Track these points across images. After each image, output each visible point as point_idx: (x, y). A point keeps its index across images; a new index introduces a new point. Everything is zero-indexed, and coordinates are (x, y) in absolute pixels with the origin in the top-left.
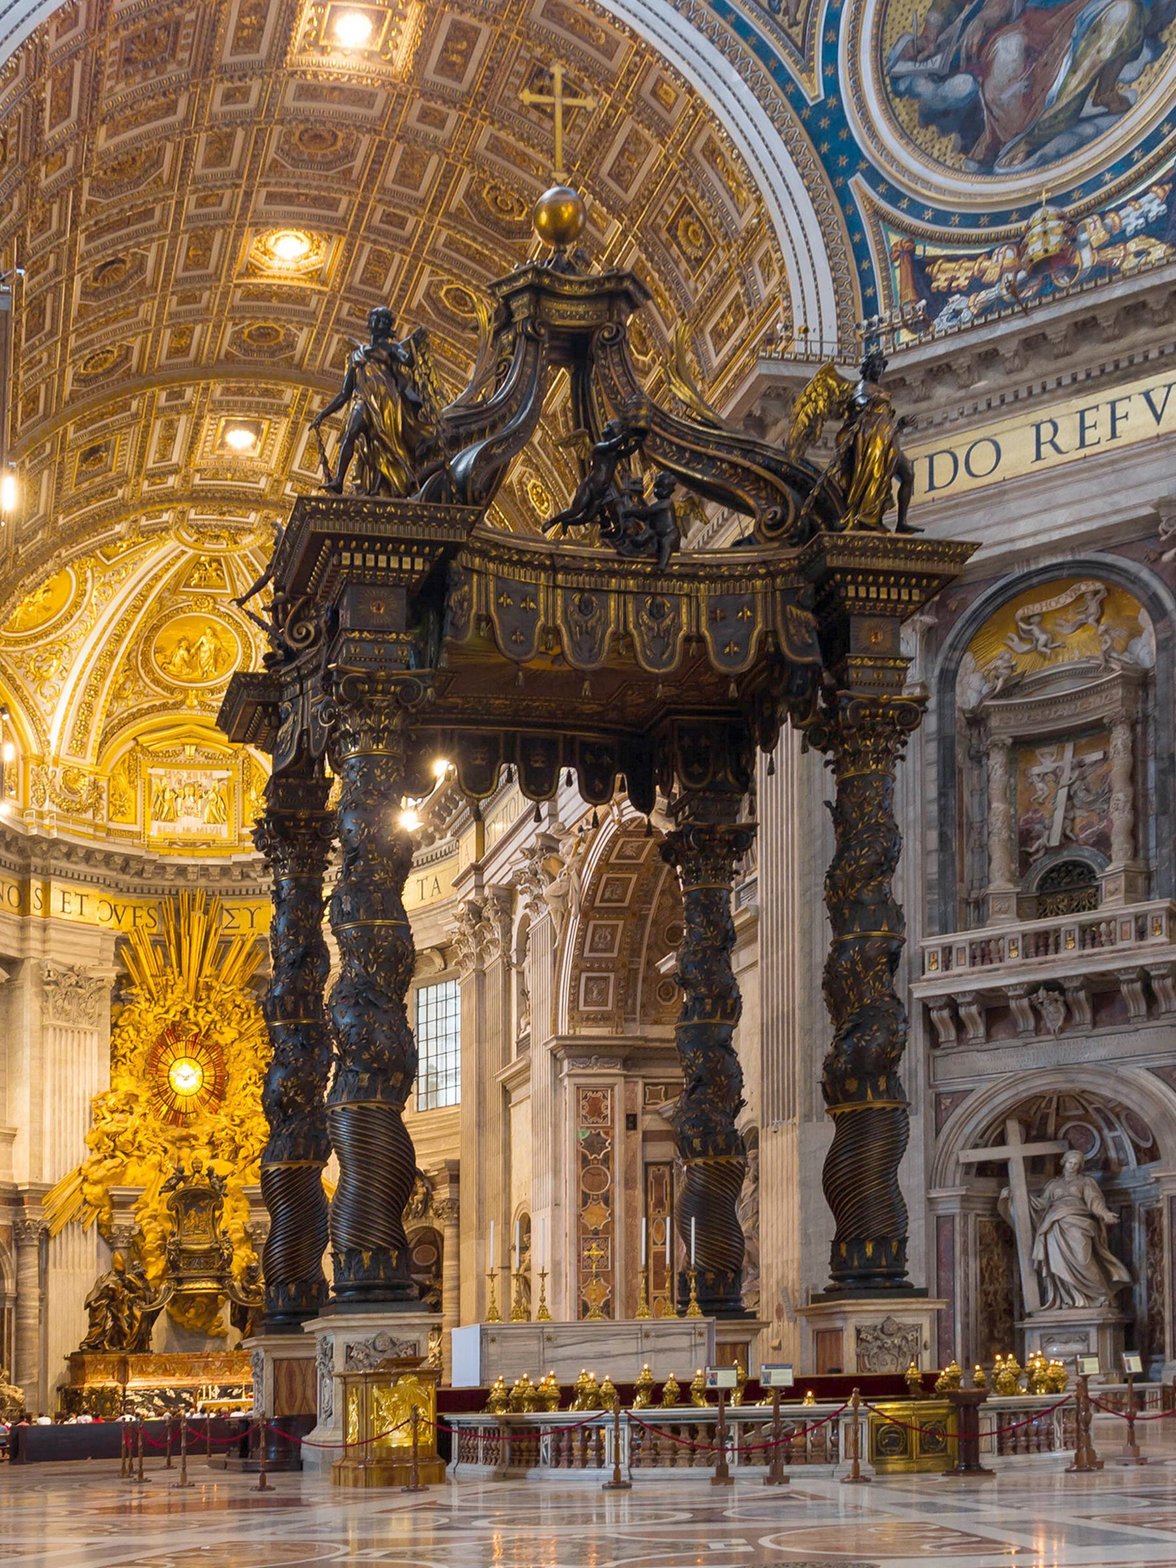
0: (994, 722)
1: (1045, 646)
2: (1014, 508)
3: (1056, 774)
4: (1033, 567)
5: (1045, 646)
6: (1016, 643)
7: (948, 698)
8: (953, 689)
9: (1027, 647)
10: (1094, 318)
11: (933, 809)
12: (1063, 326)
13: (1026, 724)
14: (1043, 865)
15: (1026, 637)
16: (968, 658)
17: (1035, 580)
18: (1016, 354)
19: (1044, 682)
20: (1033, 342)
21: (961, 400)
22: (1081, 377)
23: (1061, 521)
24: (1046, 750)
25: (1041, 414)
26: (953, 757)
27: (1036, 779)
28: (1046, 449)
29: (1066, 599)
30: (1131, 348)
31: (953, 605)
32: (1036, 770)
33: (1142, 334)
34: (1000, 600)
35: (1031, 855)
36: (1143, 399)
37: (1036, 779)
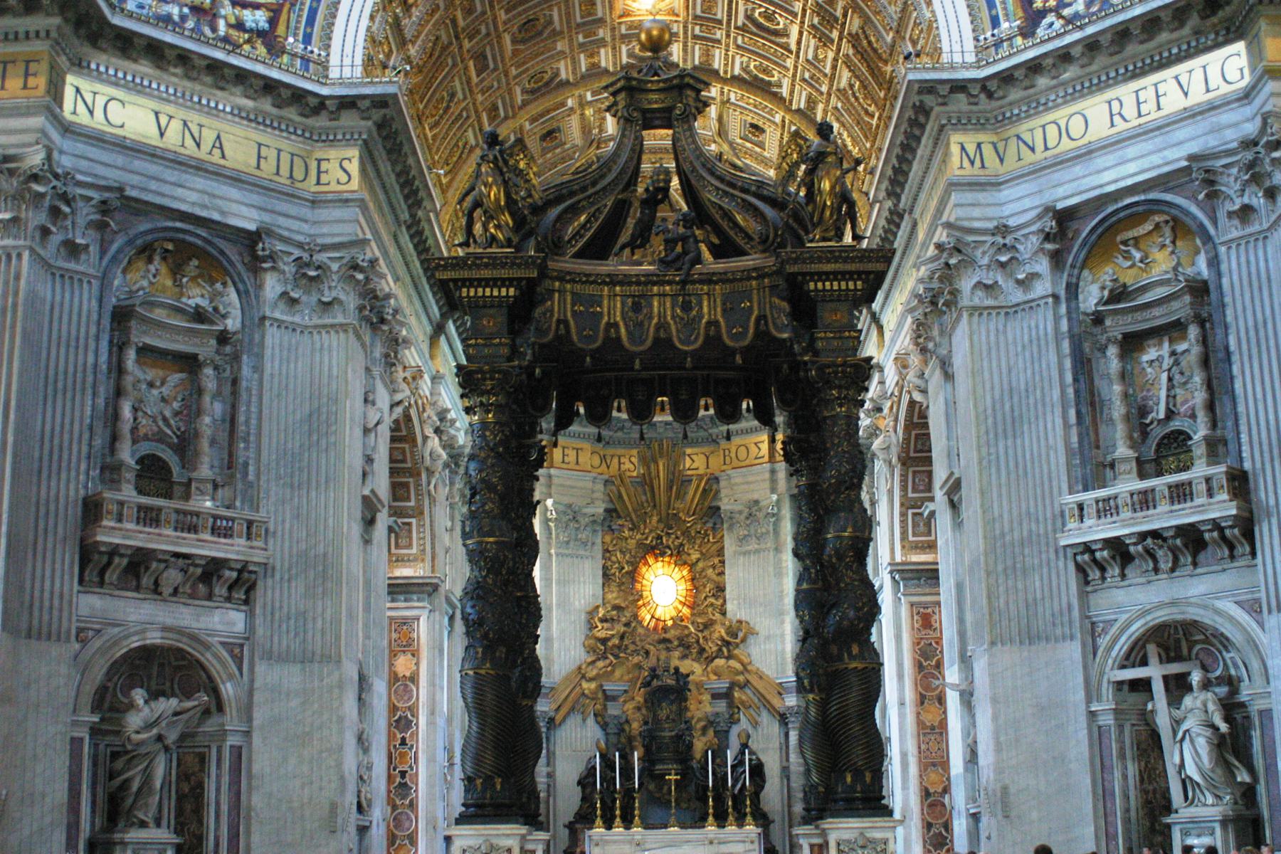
0: (1108, 322)
1: (1141, 261)
2: (1101, 161)
3: (1160, 359)
4: (1120, 205)
5: (1141, 261)
6: (1120, 260)
7: (1073, 305)
8: (1077, 298)
9: (1129, 263)
10: (1128, 29)
11: (1070, 391)
12: (1109, 36)
13: (1130, 324)
14: (1157, 433)
15: (1127, 256)
16: (1086, 273)
17: (1122, 214)
18: (1083, 54)
19: (1144, 289)
20: (1092, 45)
21: (1055, 87)
22: (1131, 68)
23: (1132, 171)
24: (1151, 342)
25: (1110, 94)
26: (1081, 352)
27: (1145, 365)
28: (1117, 119)
29: (1148, 227)
30: (1160, 46)
31: (1070, 235)
32: (1145, 358)
33: (1164, 36)
34: (1100, 230)
35: (1148, 425)
36: (1174, 81)
37: (1145, 365)
